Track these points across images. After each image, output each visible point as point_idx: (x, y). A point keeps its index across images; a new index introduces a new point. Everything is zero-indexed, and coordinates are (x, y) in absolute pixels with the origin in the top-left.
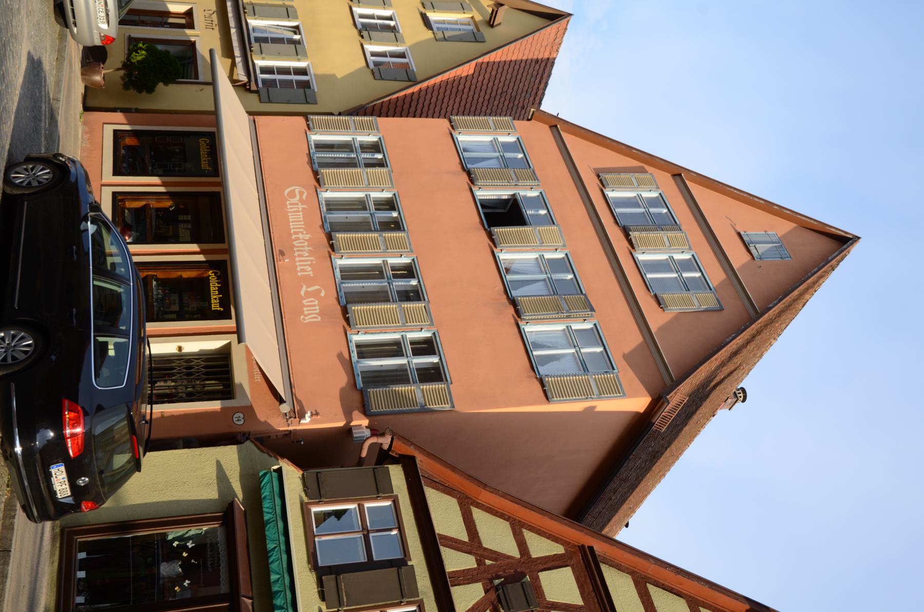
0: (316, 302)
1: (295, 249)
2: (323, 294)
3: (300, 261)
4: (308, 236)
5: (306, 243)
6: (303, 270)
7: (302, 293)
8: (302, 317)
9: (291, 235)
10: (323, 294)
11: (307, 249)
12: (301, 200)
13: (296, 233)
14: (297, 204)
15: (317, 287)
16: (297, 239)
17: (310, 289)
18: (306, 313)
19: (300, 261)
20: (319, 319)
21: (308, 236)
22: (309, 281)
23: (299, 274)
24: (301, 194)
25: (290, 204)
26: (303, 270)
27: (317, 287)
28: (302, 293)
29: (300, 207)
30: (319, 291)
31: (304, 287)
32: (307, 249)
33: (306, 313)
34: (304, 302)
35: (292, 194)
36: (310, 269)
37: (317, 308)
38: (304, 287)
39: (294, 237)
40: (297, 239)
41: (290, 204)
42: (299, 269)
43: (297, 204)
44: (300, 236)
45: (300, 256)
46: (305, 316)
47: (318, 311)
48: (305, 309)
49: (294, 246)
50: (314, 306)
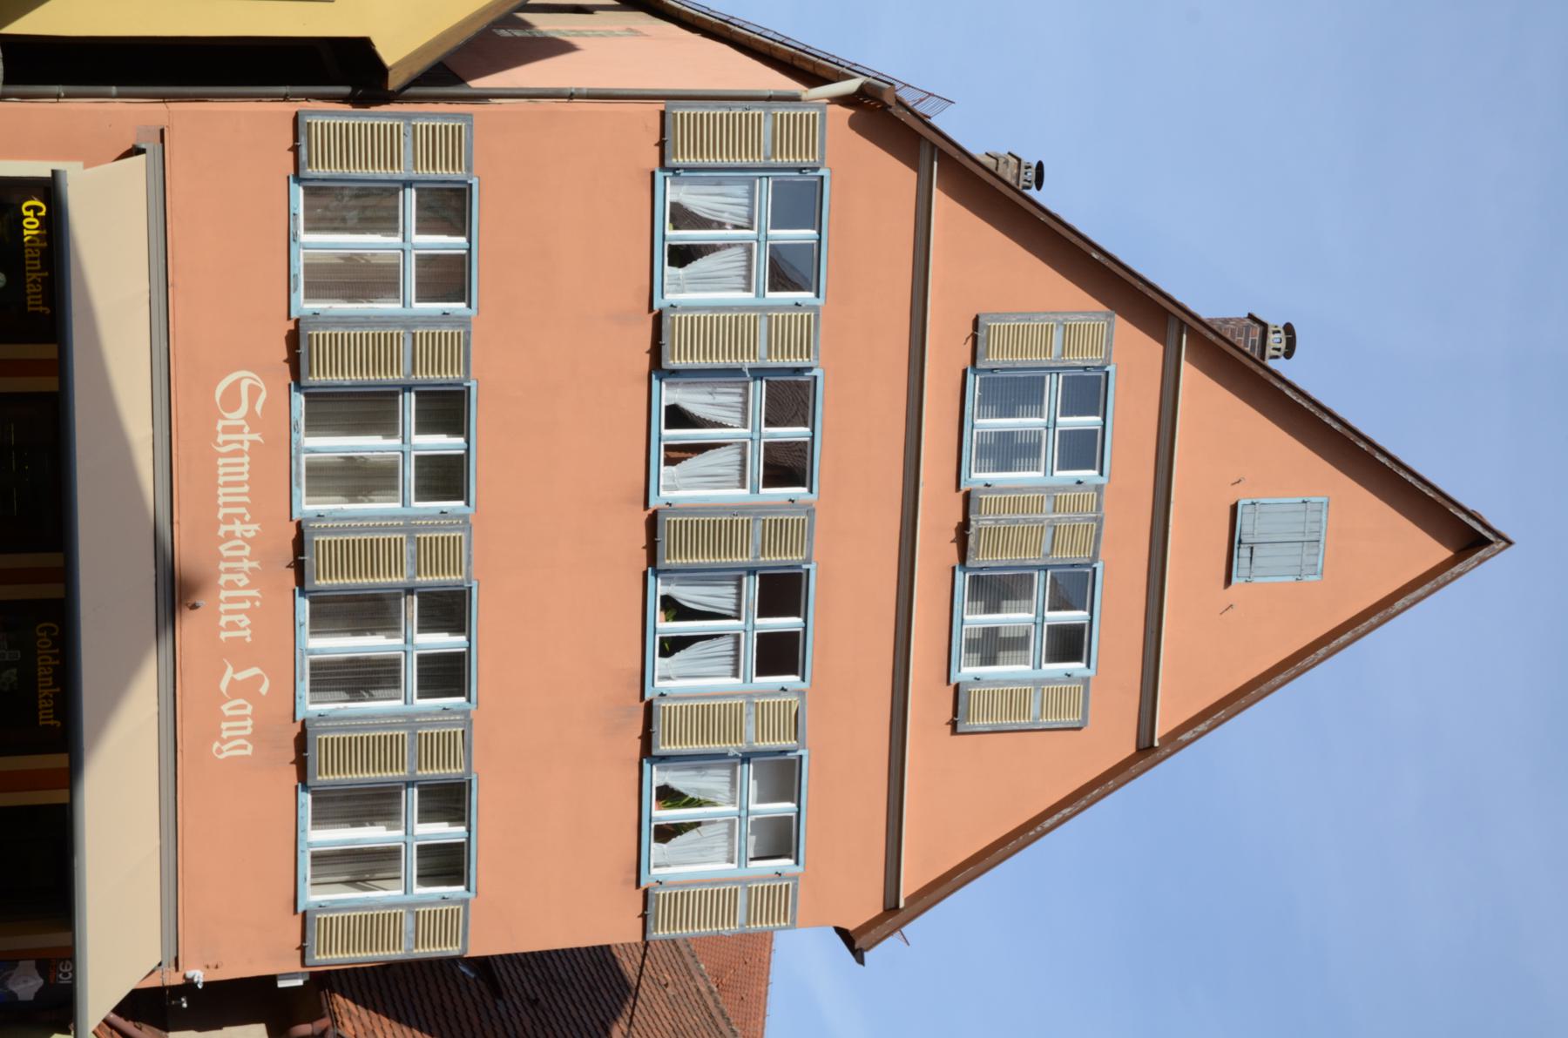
0: (249, 710)
2: (264, 690)
3: (230, 600)
4: (252, 530)
5: (247, 551)
6: (232, 626)
7: (224, 686)
8: (216, 745)
9: (217, 524)
10: (264, 690)
11: (246, 565)
12: (250, 416)
13: (229, 519)
14: (239, 430)
15: (255, 671)
17: (240, 676)
18: (225, 735)
19: (230, 600)
20: (249, 751)
22: (240, 654)
23: (223, 635)
24: (254, 392)
25: (227, 430)
26: (232, 626)
27: (255, 671)
28: (224, 686)
29: (248, 437)
30: (257, 680)
31: (230, 670)
32: (246, 565)
33: (225, 735)
34: (225, 708)
36: (247, 622)
37: (249, 722)
38: (230, 670)
39: (223, 529)
41: (227, 430)
42: (223, 621)
43: (239, 430)
44: (238, 528)
45: (231, 585)
46: (224, 742)
47: (249, 731)
48: (224, 725)
50: (243, 718)
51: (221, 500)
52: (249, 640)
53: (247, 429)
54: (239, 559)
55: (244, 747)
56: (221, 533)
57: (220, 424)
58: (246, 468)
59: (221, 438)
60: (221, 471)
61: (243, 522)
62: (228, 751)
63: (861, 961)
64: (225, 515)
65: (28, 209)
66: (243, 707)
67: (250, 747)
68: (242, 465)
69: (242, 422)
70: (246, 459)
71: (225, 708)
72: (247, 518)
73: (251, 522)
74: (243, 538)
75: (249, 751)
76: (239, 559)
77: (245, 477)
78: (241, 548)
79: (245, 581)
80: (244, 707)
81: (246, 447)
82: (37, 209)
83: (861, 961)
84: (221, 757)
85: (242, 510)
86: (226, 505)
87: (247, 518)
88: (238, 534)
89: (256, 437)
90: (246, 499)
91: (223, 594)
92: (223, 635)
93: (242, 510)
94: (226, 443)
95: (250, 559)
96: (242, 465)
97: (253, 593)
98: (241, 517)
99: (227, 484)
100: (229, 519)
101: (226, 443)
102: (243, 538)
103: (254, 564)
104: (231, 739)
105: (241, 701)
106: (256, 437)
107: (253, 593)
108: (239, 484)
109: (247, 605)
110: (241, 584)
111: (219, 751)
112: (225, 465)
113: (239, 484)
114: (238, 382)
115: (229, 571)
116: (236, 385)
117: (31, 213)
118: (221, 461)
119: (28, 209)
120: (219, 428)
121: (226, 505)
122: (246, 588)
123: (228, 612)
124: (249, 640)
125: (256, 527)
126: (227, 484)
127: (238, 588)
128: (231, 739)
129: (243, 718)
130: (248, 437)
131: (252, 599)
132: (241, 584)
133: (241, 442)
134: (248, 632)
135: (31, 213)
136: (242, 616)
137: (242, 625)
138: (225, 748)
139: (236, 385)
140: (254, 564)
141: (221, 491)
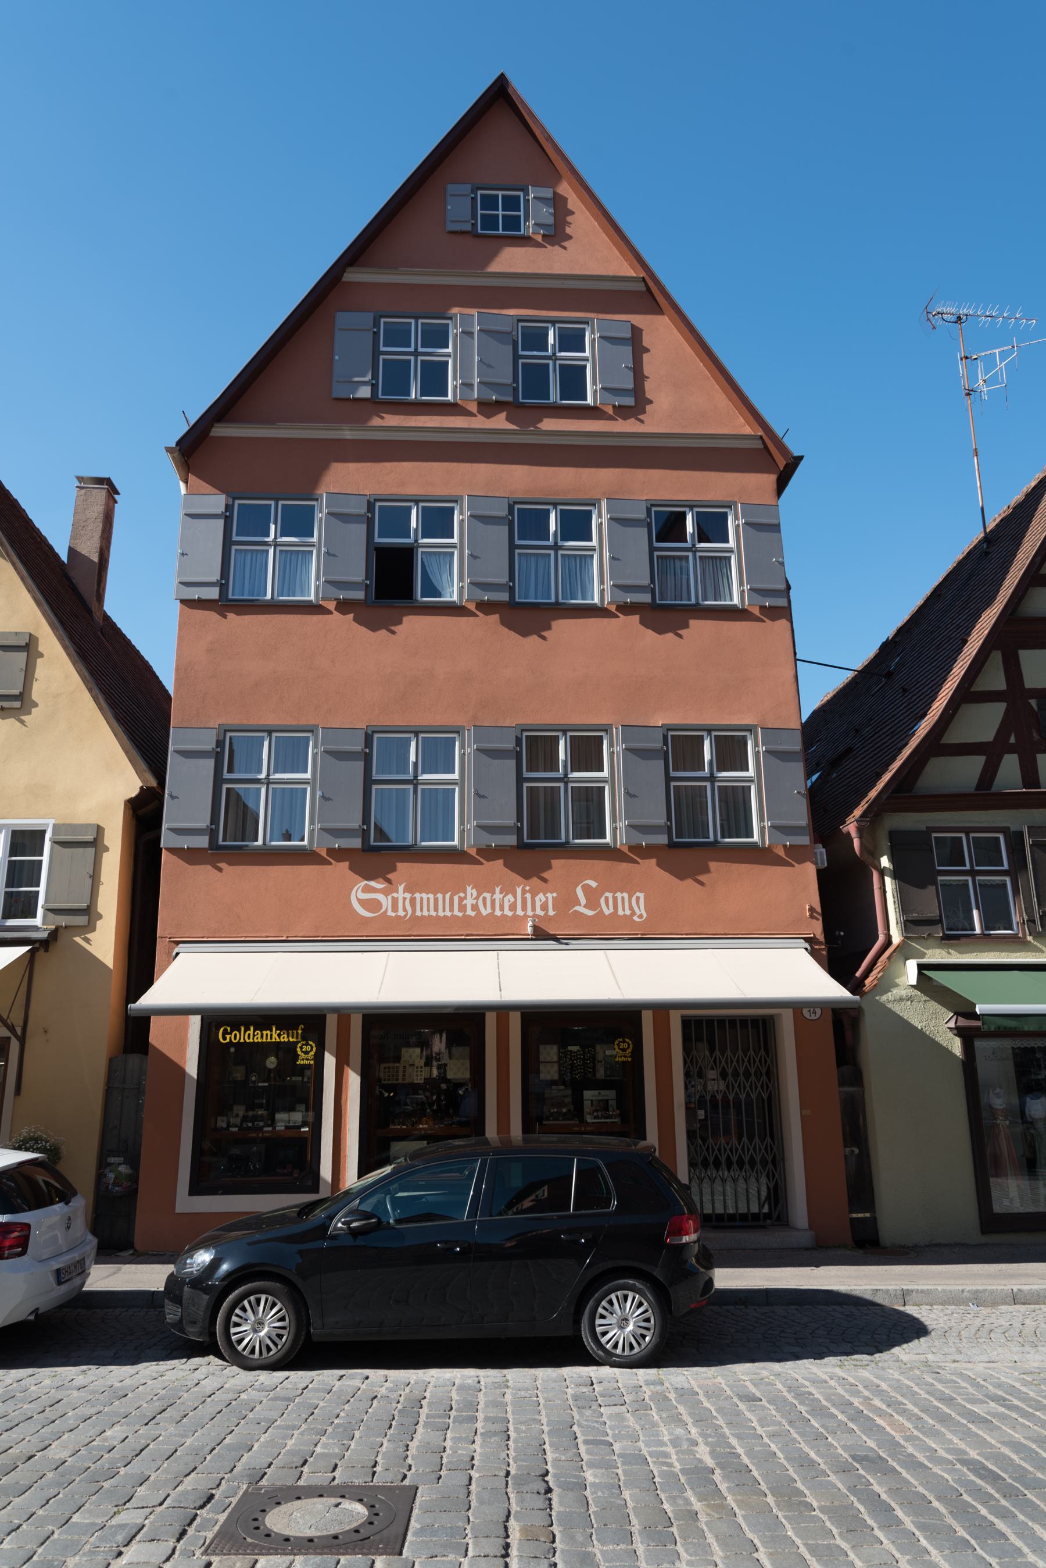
0: (609, 895)
1: (498, 913)
3: (524, 908)
4: (471, 891)
5: (488, 895)
6: (544, 907)
7: (590, 913)
8: (636, 918)
11: (498, 896)
12: (386, 892)
14: (395, 901)
15: (579, 891)
16: (475, 907)
17: (583, 900)
18: (628, 912)
19: (524, 908)
20: (641, 895)
21: (471, 891)
23: (551, 913)
24: (367, 889)
25: (395, 908)
26: (544, 907)
27: (579, 891)
28: (590, 913)
29: (401, 894)
30: (586, 889)
31: (577, 908)
32: (498, 896)
33: (628, 912)
34: (607, 912)
35: (372, 905)
36: (541, 896)
37: (619, 895)
38: (577, 908)
39: (470, 912)
40: (475, 907)
41: (395, 908)
43: (395, 901)
44: (469, 902)
45: (513, 907)
46: (633, 913)
48: (620, 912)
49: (492, 914)
50: (615, 899)
51: (448, 913)
52: (555, 895)
53: (395, 895)
54: (493, 902)
55: (638, 899)
56: (473, 914)
57: (390, 913)
58: (424, 896)
59: (401, 913)
60: (425, 913)
61: (465, 898)
62: (641, 910)
63: (801, 458)
64: (459, 911)
65: (225, 1039)
66: (607, 899)
67: (638, 894)
68: (422, 899)
69: (390, 897)
70: (417, 895)
71: (607, 912)
72: (462, 895)
73: (465, 892)
74: (477, 898)
75: (641, 895)
76: (493, 902)
77: (431, 896)
78: (485, 899)
79: (510, 897)
80: (607, 899)
81: (408, 896)
82: (225, 1033)
83: (801, 458)
84: (645, 915)
85: (456, 898)
86: (452, 909)
87: (462, 895)
88: (474, 902)
89: (401, 888)
90: (448, 896)
91: (520, 912)
92: (551, 913)
93: (456, 898)
94: (405, 910)
95: (494, 893)
96: (422, 899)
97: (519, 891)
98: (461, 899)
99: (436, 909)
100: (462, 908)
101: (405, 910)
102: (477, 898)
103: (498, 890)
104: (631, 908)
105: (602, 901)
106: (401, 888)
107: (519, 891)
108: (436, 900)
109: (528, 896)
110: (512, 900)
111: (641, 916)
112: (422, 910)
113: (436, 900)
114: (358, 899)
115: (502, 908)
116: (362, 903)
117: (228, 1037)
118: (418, 913)
119: (225, 1039)
120: (393, 914)
121: (452, 909)
122: (515, 897)
123: (534, 909)
124: (555, 895)
125: (469, 889)
126: (436, 909)
127: (515, 902)
128: (631, 908)
129: (615, 899)
130: (401, 894)
131: (524, 892)
132: (512, 900)
133: (404, 899)
134: (549, 895)
135: (228, 1037)
136: (537, 899)
137: (543, 899)
138: (638, 913)
139: (362, 903)
140: (498, 890)
141: (441, 914)
